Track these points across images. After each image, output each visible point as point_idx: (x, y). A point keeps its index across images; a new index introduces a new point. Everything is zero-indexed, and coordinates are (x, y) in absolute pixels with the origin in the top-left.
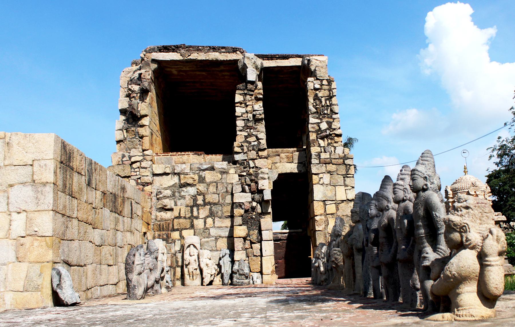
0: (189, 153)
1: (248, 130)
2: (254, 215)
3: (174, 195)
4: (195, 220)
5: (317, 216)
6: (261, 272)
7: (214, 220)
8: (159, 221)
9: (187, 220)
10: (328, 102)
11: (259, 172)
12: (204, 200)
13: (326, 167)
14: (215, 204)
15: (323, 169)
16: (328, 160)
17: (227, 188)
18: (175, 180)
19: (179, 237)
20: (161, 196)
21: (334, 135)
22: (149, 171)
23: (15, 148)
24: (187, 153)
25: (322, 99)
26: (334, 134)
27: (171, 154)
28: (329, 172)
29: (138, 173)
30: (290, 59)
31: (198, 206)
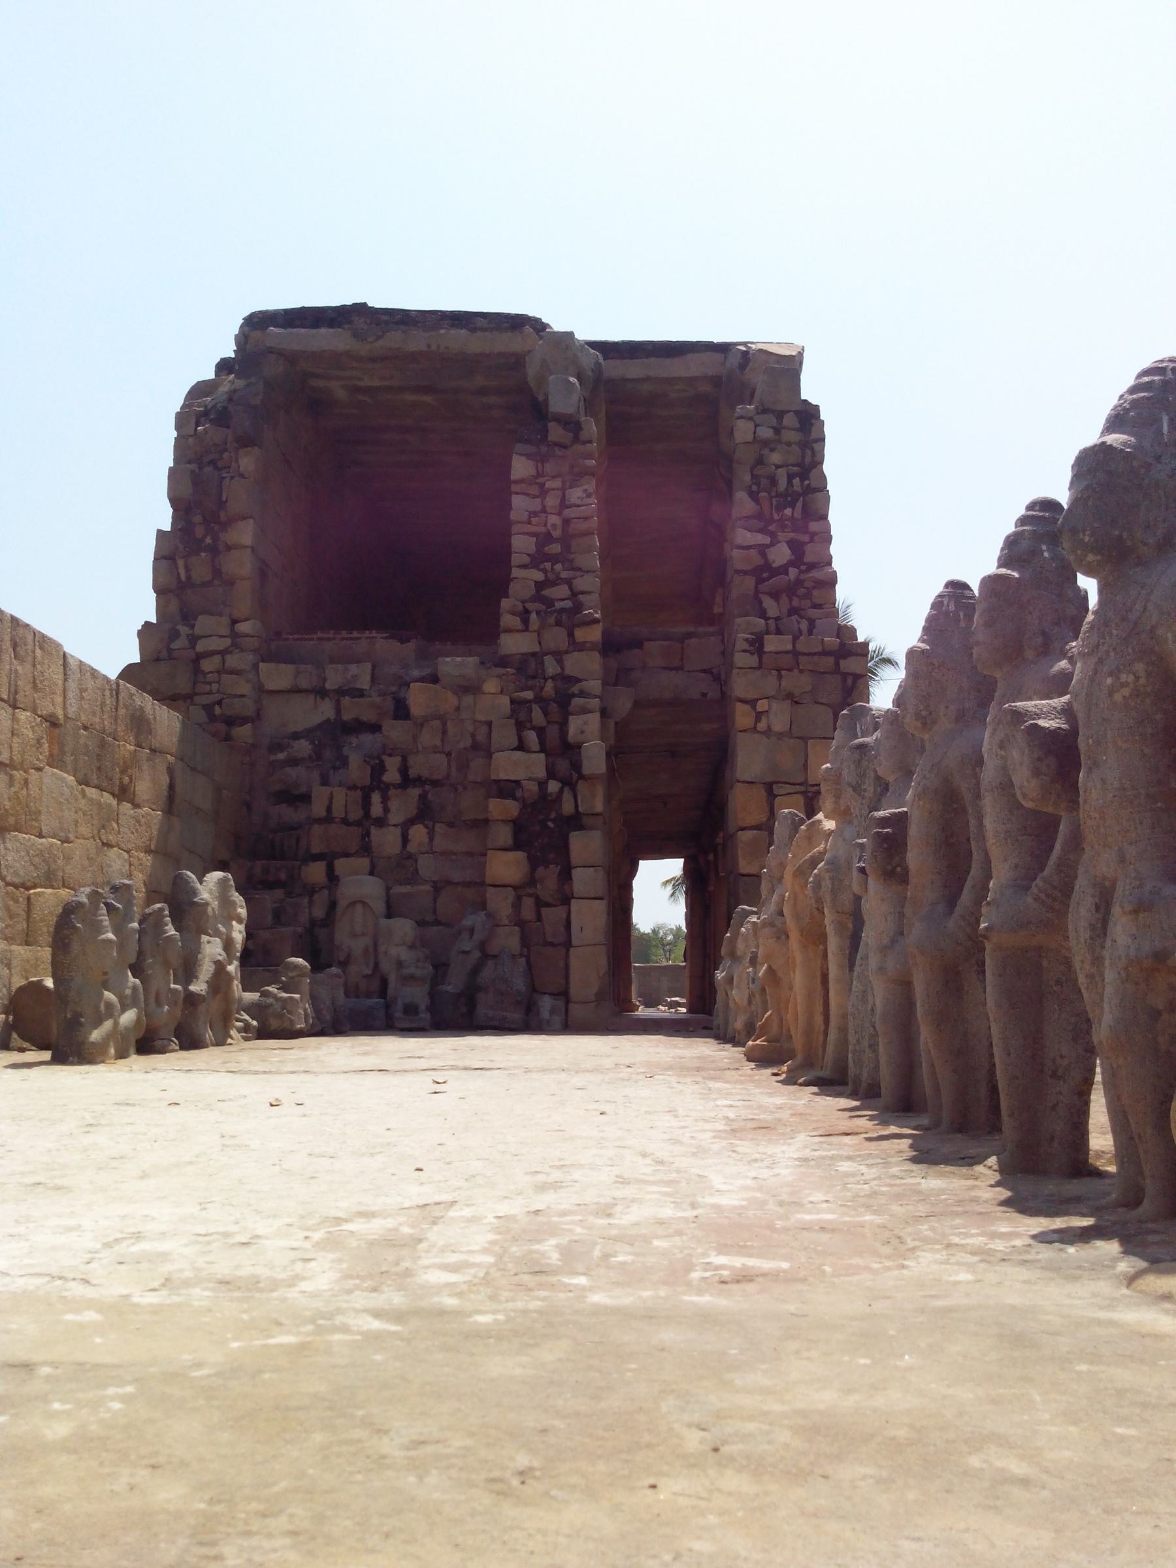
0: (374, 635)
1: (548, 565)
2: (553, 820)
3: (317, 755)
4: (374, 831)
5: (743, 829)
6: (564, 995)
9: (352, 828)
10: (796, 481)
11: (575, 689)
12: (404, 770)
13: (780, 677)
14: (435, 783)
18: (326, 710)
20: (281, 756)
21: (813, 584)
22: (248, 681)
24: (367, 634)
27: (320, 635)
28: (789, 696)
29: (215, 687)
30: (689, 356)
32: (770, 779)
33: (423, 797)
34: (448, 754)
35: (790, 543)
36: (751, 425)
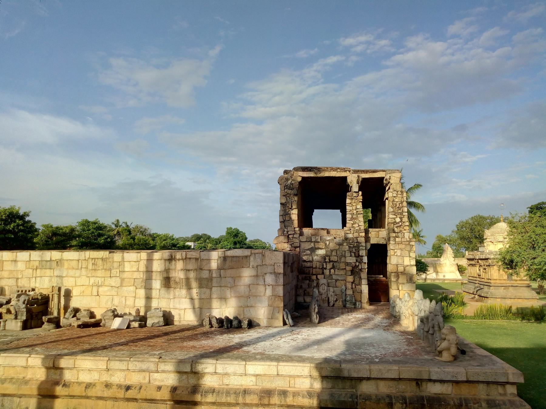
1: (354, 220)
7: (335, 271)
8: (304, 268)
10: (401, 205)
11: (360, 245)
12: (329, 259)
14: (335, 262)
15: (397, 247)
16: (400, 242)
17: (342, 253)
19: (316, 279)
23: (267, 258)
27: (308, 229)
28: (401, 249)
31: (326, 262)
33: (333, 264)
34: (338, 257)
36: (392, 193)
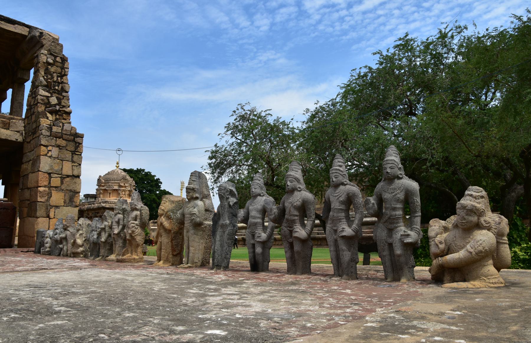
5: (40, 187)
13: (56, 140)
25: (55, 74)
26: (64, 111)
30: (16, 25)
32: (50, 171)
35: (57, 98)
36: (45, 57)
